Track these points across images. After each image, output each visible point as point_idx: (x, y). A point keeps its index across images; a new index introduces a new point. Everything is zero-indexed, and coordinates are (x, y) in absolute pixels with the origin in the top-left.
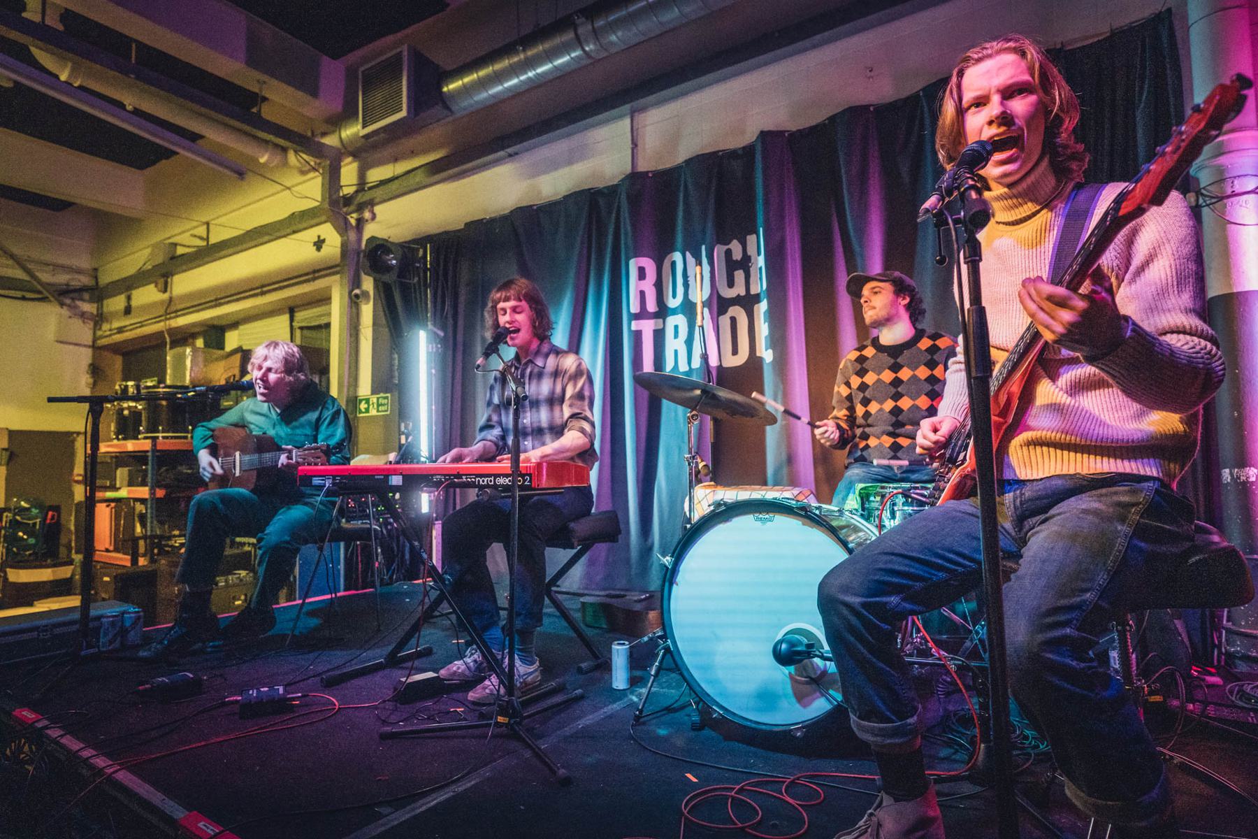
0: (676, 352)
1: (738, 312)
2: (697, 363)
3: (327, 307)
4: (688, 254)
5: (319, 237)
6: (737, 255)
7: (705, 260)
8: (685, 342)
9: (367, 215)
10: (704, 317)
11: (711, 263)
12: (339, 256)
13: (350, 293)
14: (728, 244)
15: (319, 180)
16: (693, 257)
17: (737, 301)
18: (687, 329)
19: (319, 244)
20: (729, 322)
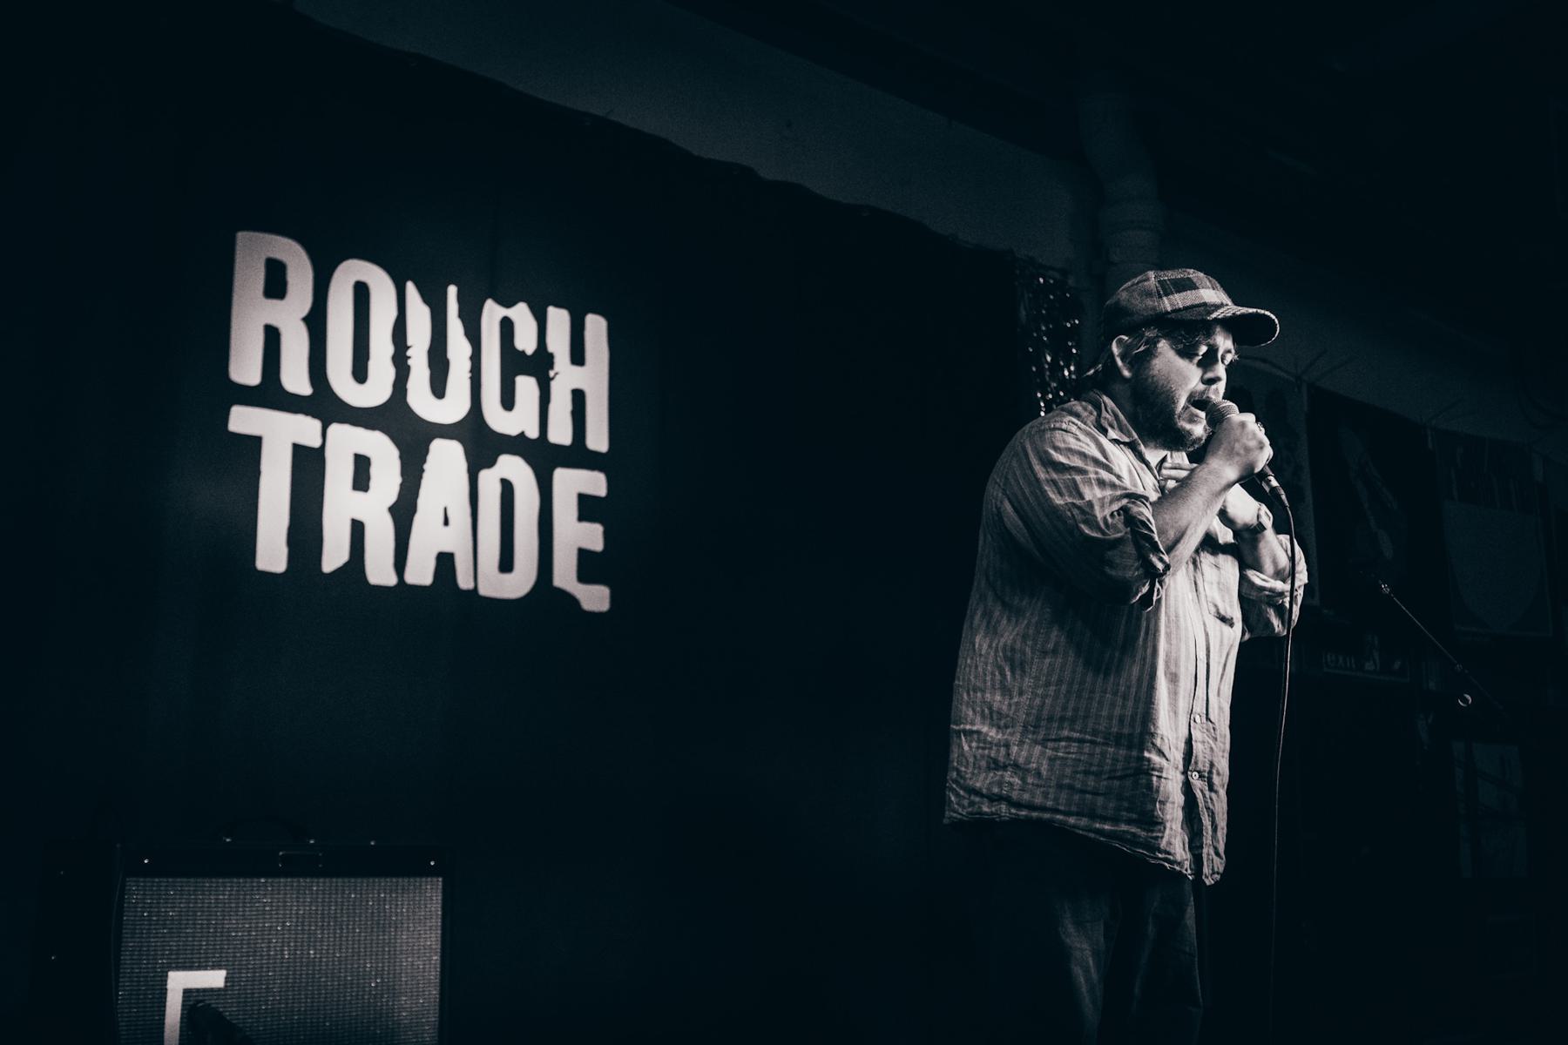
0: (358, 529)
1: (513, 467)
2: (421, 572)
6: (526, 341)
7: (455, 327)
8: (393, 510)
10: (446, 458)
11: (473, 335)
14: (508, 304)
17: (518, 445)
18: (398, 480)
20: (497, 489)
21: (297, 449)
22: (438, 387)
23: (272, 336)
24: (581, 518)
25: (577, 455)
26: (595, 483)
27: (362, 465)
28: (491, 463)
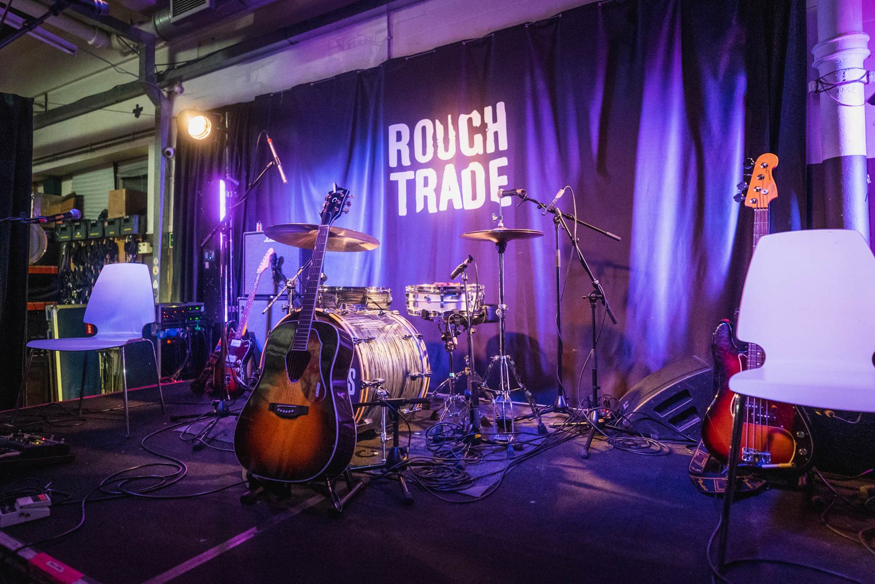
0: (426, 198)
2: (443, 207)
3: (144, 162)
4: (437, 122)
5: (137, 106)
6: (477, 123)
8: (435, 190)
9: (177, 89)
10: (450, 170)
12: (154, 122)
13: (163, 151)
15: (138, 59)
16: (441, 123)
17: (476, 158)
18: (436, 181)
19: (138, 111)
20: (470, 174)
21: (408, 181)
22: (446, 149)
23: (399, 152)
24: (499, 176)
25: (498, 154)
26: (503, 162)
27: (426, 179)
28: (466, 166)
